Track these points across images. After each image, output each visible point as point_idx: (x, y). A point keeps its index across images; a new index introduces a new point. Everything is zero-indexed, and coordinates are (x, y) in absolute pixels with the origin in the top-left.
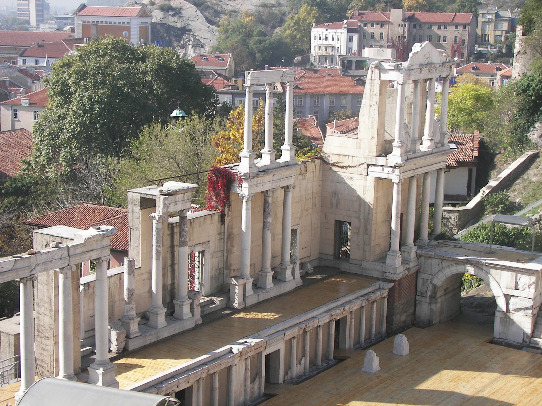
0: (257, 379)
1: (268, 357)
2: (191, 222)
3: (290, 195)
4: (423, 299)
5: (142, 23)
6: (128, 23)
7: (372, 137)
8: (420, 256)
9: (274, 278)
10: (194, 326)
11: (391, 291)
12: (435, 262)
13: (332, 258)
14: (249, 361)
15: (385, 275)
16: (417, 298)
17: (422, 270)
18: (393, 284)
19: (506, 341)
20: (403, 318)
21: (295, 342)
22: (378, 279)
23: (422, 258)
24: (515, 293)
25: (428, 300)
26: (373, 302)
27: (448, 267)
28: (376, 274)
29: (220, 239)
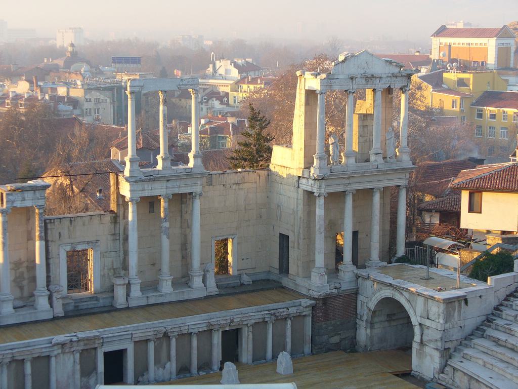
0: (94, 374)
1: (107, 355)
2: (71, 221)
4: (361, 322)
5: (502, 44)
6: (485, 44)
7: (301, 149)
9: (175, 284)
10: (52, 317)
11: (314, 308)
13: (277, 272)
14: (78, 355)
16: (358, 321)
19: (420, 375)
20: (335, 339)
21: (151, 346)
22: (305, 296)
25: (364, 324)
26: (286, 318)
28: (304, 292)
29: (115, 240)
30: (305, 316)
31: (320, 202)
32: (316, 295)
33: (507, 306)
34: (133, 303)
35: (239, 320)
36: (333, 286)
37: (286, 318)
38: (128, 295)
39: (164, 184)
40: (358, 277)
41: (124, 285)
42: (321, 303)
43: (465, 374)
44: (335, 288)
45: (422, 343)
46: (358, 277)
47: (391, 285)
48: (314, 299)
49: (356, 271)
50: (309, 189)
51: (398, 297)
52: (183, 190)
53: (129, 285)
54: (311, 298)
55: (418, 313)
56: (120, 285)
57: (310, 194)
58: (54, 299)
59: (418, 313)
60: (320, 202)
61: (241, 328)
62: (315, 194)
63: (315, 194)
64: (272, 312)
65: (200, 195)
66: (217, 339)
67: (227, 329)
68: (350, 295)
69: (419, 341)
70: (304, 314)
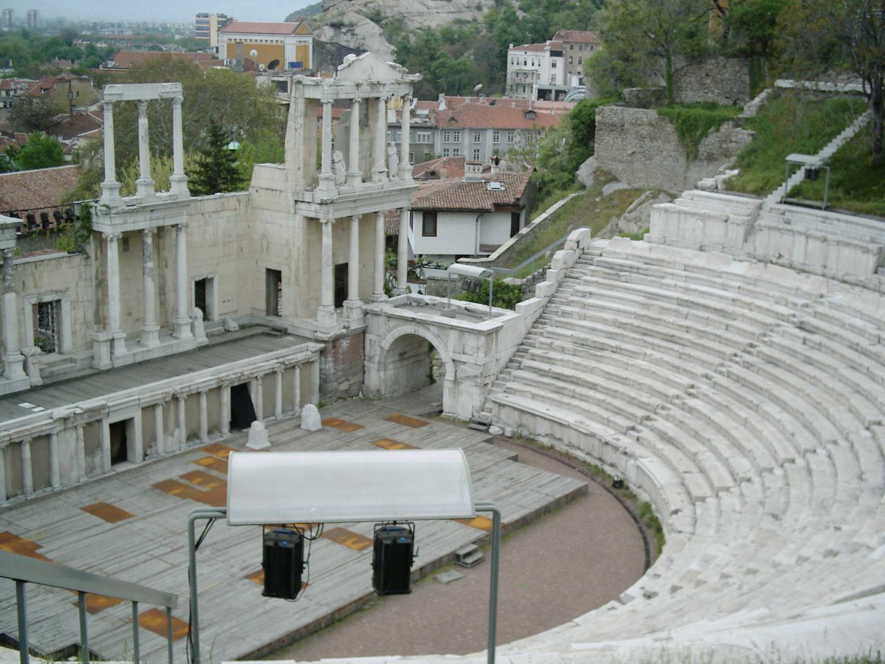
3: (183, 237)
8: (367, 313)
12: (382, 319)
15: (316, 334)
17: (369, 330)
18: (322, 345)
22: (310, 340)
23: (369, 316)
24: (463, 358)
26: (294, 367)
27: (395, 327)
30: (313, 362)
31: (327, 230)
32: (325, 337)
33: (536, 334)
34: (119, 363)
35: (249, 372)
36: (342, 325)
37: (294, 367)
38: (112, 353)
39: (148, 215)
40: (366, 313)
41: (107, 341)
42: (330, 345)
43: (515, 409)
44: (345, 328)
45: (456, 381)
46: (366, 313)
47: (414, 320)
48: (322, 341)
49: (365, 307)
50: (313, 215)
51: (422, 332)
52: (168, 222)
53: (112, 341)
54: (318, 341)
55: (451, 348)
56: (103, 342)
57: (313, 222)
58: (30, 364)
59: (451, 348)
60: (327, 230)
61: (250, 382)
62: (321, 221)
63: (321, 221)
64: (281, 360)
65: (187, 226)
66: (226, 397)
67: (236, 384)
68: (358, 335)
69: (452, 379)
70: (312, 360)
